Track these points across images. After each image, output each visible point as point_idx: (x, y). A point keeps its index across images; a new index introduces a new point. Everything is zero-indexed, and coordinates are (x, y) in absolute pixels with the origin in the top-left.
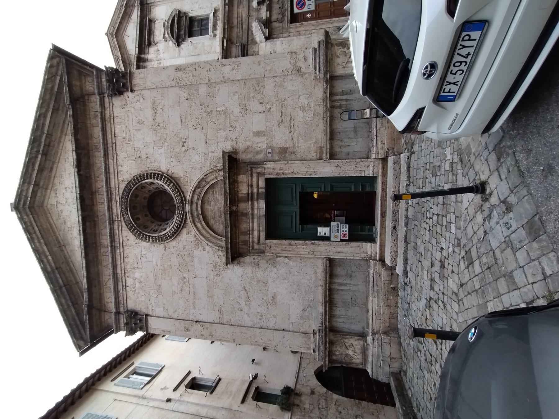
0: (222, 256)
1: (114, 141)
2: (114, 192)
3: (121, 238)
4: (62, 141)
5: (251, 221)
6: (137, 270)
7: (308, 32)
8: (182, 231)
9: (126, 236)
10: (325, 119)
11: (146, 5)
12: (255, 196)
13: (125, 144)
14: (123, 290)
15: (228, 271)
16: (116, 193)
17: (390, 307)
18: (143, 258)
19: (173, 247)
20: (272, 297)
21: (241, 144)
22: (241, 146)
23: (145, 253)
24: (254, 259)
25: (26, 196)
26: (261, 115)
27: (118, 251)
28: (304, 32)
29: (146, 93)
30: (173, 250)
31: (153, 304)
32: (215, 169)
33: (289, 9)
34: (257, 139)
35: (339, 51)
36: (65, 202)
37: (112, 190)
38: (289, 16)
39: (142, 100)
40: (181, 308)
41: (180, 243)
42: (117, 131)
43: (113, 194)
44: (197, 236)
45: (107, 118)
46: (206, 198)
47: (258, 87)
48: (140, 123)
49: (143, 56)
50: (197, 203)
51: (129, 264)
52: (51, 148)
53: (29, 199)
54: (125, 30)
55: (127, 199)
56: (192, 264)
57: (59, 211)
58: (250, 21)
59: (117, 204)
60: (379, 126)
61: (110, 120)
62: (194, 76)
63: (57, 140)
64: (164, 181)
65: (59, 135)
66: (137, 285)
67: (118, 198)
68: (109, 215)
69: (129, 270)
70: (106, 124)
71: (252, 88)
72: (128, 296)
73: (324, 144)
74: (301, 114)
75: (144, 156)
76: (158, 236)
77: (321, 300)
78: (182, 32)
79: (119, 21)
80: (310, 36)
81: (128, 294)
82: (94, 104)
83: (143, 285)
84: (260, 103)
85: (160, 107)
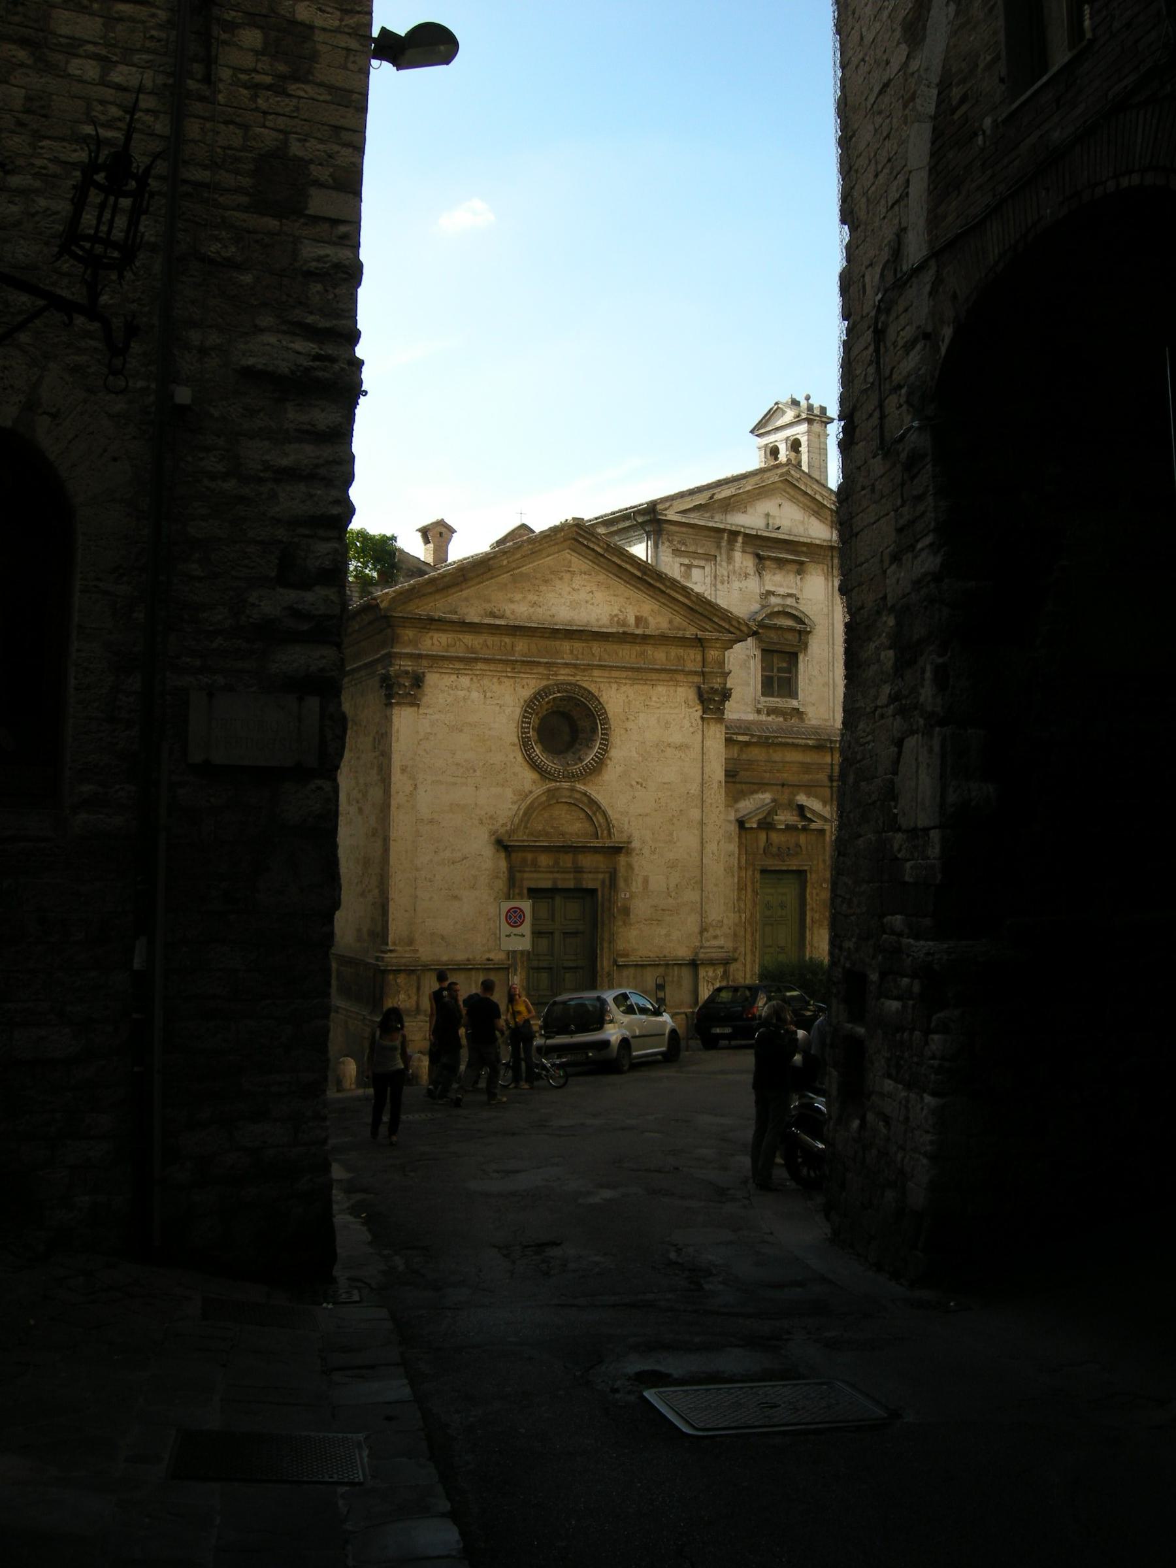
0: (506, 828)
1: (648, 682)
3: (526, 676)
4: (653, 600)
6: (482, 696)
7: (742, 906)
8: (536, 773)
9: (528, 685)
10: (657, 959)
11: (830, 554)
13: (643, 698)
14: (452, 669)
15: (486, 836)
16: (585, 676)
18: (498, 707)
19: (515, 758)
21: (636, 860)
22: (635, 861)
23: (507, 712)
24: (504, 873)
25: (589, 540)
26: (665, 886)
27: (509, 670)
28: (743, 897)
29: (699, 736)
30: (511, 756)
32: (611, 825)
33: (785, 868)
34: (640, 880)
35: (719, 973)
36: (574, 585)
37: (589, 672)
38: (773, 868)
39: (692, 730)
41: (521, 769)
43: (584, 672)
44: (531, 795)
45: (675, 675)
46: (574, 808)
47: (694, 883)
48: (667, 725)
49: (740, 539)
50: (570, 797)
52: (646, 586)
53: (585, 543)
54: (792, 499)
57: (562, 574)
58: (775, 787)
59: (572, 675)
61: (673, 681)
62: (711, 804)
63: (655, 596)
64: (599, 753)
65: (663, 601)
66: (461, 694)
67: (578, 678)
68: (558, 663)
69: (481, 682)
71: (694, 875)
72: (443, 676)
73: (632, 958)
74: (663, 932)
75: (630, 725)
77: (456, 959)
78: (772, 635)
79: (809, 492)
80: (736, 909)
81: (447, 676)
82: (691, 660)
83: (462, 704)
84: (677, 885)
85: (683, 755)
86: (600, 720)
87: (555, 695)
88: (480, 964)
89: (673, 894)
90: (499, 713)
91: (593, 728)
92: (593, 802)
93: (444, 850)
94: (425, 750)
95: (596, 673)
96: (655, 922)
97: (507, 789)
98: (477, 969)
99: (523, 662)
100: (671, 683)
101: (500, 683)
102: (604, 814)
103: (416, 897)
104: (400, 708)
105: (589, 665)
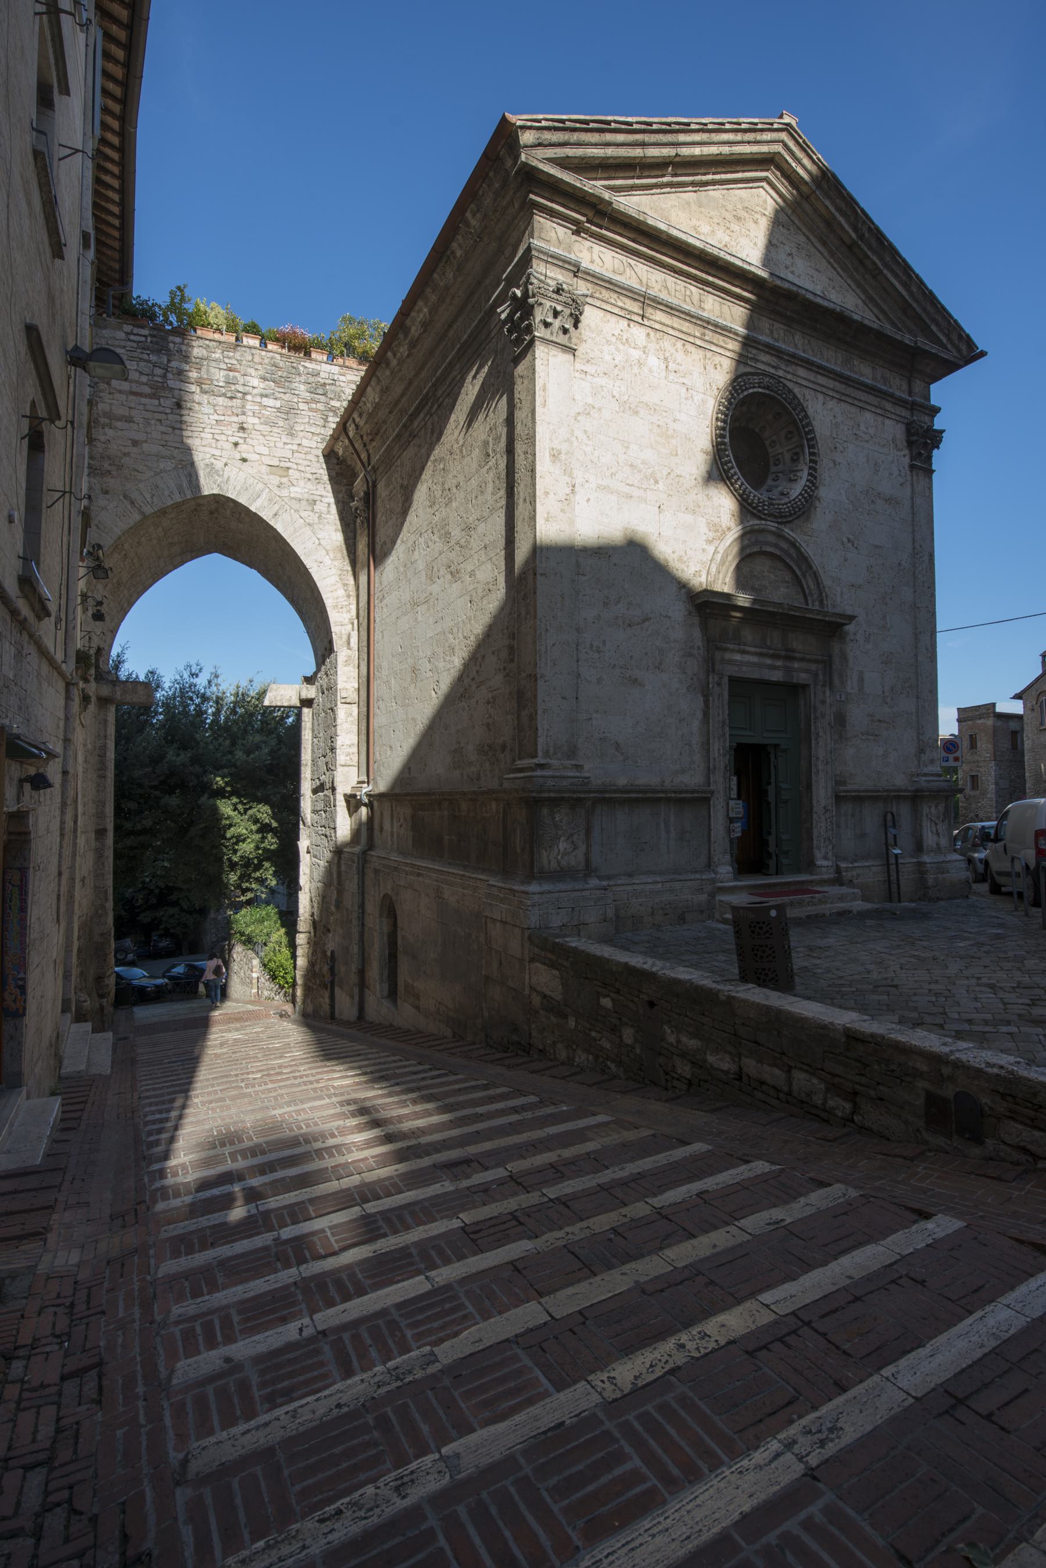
1: (856, 403)
2: (789, 369)
4: (858, 291)
5: (758, 650)
6: (663, 366)
12: (788, 664)
16: (788, 372)
17: (652, 914)
20: (636, 679)
23: (695, 398)
24: (699, 648)
31: (601, 381)
37: (794, 367)
40: (596, 453)
42: (868, 415)
45: (884, 402)
50: (776, 546)
51: (673, 351)
55: (780, 395)
56: (683, 509)
59: (773, 367)
60: (874, 869)
62: (924, 582)
66: (636, 354)
67: (781, 373)
70: (877, 396)
72: (609, 315)
73: (849, 787)
76: (724, 444)
81: (614, 318)
86: (808, 440)
87: (756, 390)
88: (675, 792)
89: (889, 700)
90: (686, 399)
91: (797, 454)
92: (803, 559)
93: (618, 602)
94: (585, 432)
95: (801, 372)
96: (871, 737)
97: (701, 519)
98: (669, 800)
99: (716, 325)
100: (879, 411)
101: (686, 352)
102: (816, 576)
103: (579, 676)
104: (546, 350)
105: (794, 356)
